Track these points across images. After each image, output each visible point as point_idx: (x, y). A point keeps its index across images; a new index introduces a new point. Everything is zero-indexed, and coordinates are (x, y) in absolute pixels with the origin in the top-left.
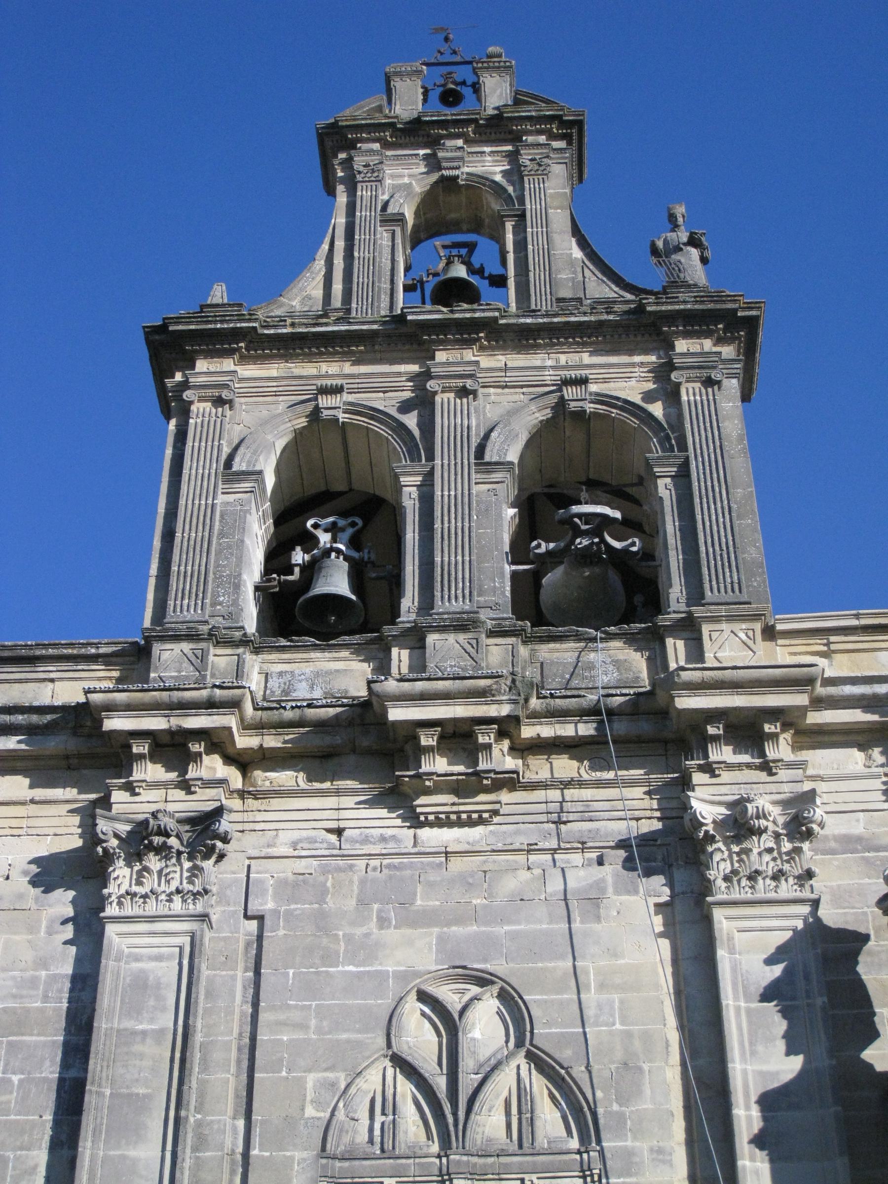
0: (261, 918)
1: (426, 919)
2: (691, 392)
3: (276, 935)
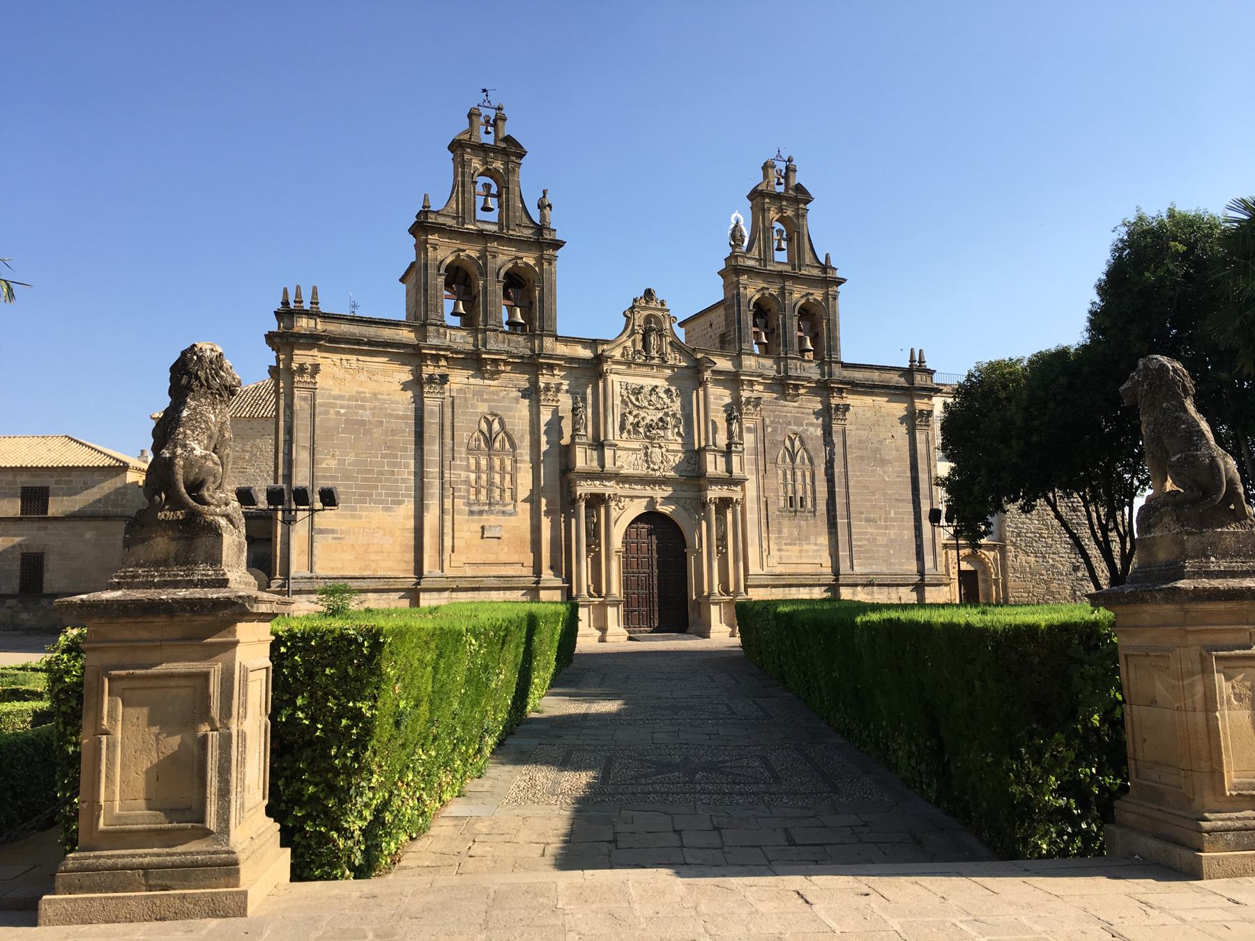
0: (453, 397)
1: (485, 401)
2: (546, 265)
3: (456, 402)
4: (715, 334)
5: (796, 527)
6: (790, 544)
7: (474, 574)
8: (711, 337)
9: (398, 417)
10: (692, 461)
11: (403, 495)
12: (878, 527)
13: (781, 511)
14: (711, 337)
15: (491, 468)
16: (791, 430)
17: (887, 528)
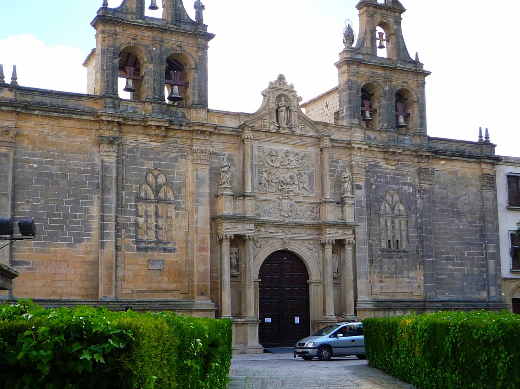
1: (152, 159)
4: (330, 113)
5: (393, 264)
6: (389, 277)
7: (141, 299)
8: (327, 115)
9: (79, 171)
10: (315, 211)
11: (84, 235)
12: (455, 265)
13: (382, 251)
14: (327, 115)
15: (156, 214)
16: (390, 188)
17: (461, 265)
